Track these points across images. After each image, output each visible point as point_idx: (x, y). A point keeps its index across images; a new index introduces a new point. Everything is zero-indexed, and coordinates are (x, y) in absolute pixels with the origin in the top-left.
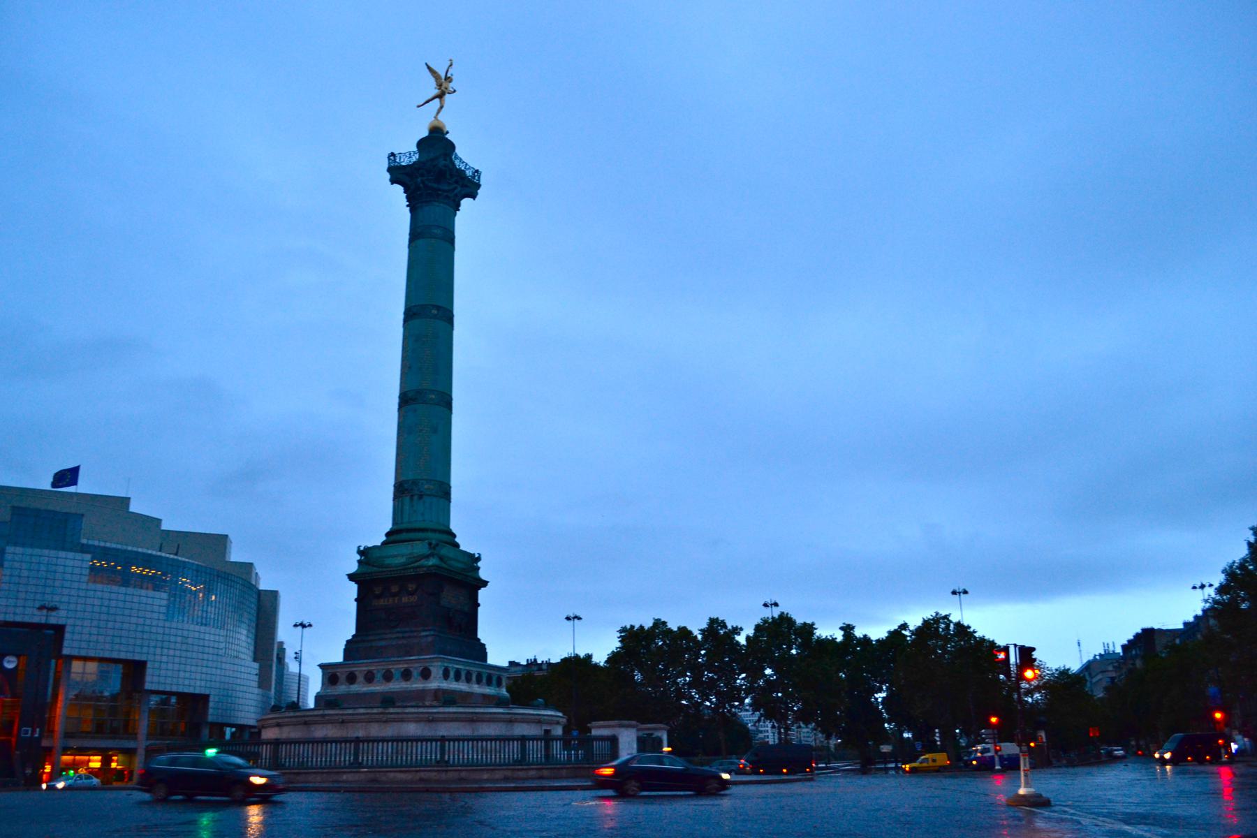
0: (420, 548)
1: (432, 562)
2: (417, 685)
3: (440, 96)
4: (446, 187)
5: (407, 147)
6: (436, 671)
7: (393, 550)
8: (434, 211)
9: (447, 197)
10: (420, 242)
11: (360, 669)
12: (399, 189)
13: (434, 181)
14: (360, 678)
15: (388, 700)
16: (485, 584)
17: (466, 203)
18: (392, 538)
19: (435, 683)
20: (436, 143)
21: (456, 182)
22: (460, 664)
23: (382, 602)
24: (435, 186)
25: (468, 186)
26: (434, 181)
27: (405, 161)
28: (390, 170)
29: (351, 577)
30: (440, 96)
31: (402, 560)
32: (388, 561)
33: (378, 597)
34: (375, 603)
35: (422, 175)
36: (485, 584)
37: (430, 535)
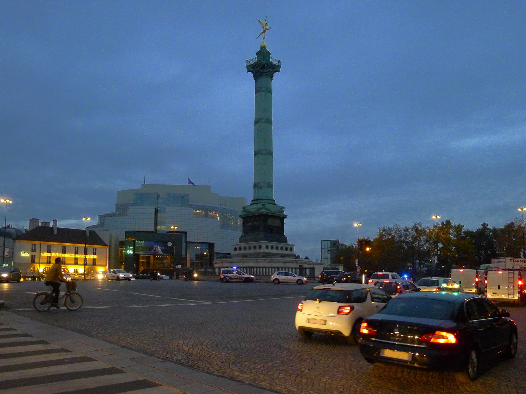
0: (260, 206)
1: (263, 210)
2: (257, 251)
3: (264, 32)
4: (265, 71)
5: (253, 58)
6: (263, 246)
7: (253, 206)
8: (263, 80)
9: (267, 75)
10: (257, 94)
11: (243, 245)
12: (251, 75)
13: (263, 69)
14: (243, 249)
15: (245, 256)
16: (286, 216)
17: (275, 75)
18: (254, 202)
19: (264, 250)
20: (263, 53)
21: (270, 68)
22: (280, 245)
23: (249, 224)
24: (262, 71)
25: (276, 68)
26: (263, 69)
27: (252, 63)
28: (247, 67)
29: (240, 216)
30: (264, 32)
31: (254, 210)
32: (251, 211)
33: (248, 222)
34: (247, 225)
35: (257, 68)
36: (286, 216)
37: (263, 201)
